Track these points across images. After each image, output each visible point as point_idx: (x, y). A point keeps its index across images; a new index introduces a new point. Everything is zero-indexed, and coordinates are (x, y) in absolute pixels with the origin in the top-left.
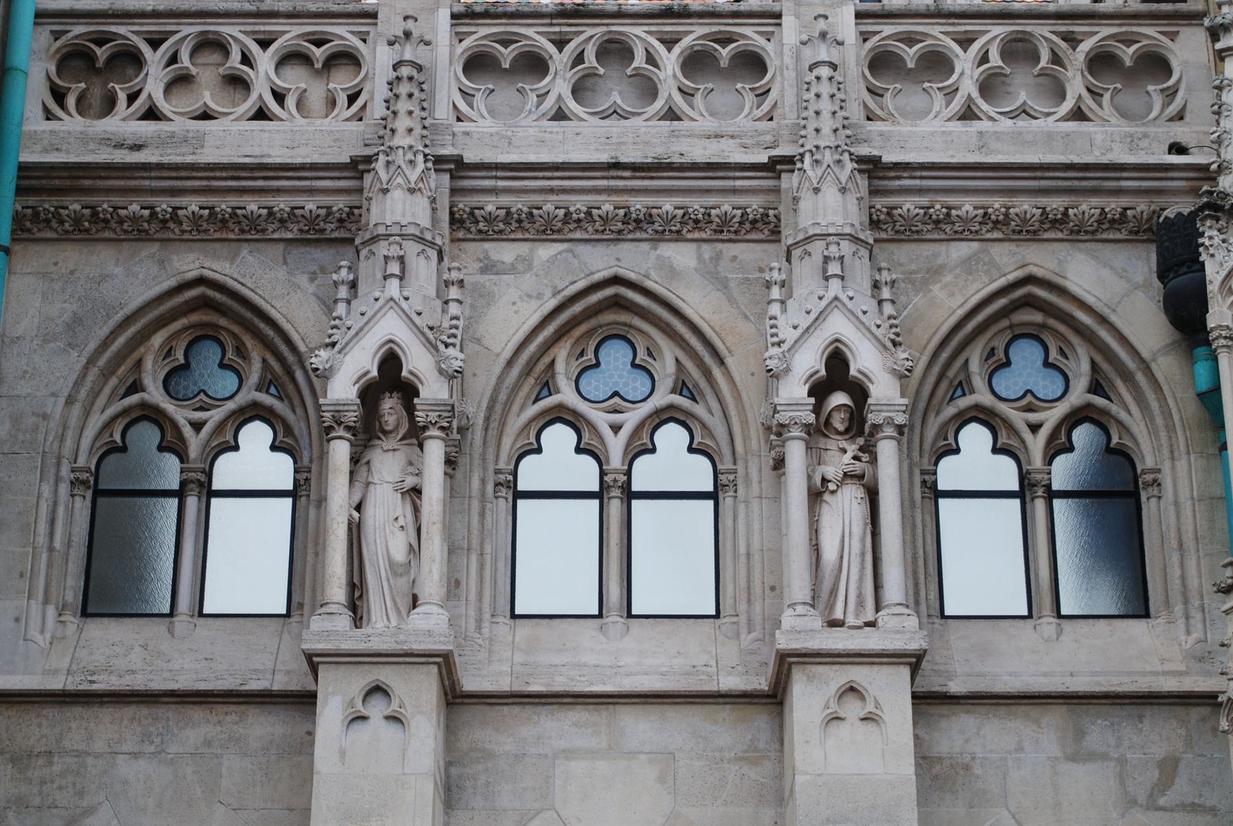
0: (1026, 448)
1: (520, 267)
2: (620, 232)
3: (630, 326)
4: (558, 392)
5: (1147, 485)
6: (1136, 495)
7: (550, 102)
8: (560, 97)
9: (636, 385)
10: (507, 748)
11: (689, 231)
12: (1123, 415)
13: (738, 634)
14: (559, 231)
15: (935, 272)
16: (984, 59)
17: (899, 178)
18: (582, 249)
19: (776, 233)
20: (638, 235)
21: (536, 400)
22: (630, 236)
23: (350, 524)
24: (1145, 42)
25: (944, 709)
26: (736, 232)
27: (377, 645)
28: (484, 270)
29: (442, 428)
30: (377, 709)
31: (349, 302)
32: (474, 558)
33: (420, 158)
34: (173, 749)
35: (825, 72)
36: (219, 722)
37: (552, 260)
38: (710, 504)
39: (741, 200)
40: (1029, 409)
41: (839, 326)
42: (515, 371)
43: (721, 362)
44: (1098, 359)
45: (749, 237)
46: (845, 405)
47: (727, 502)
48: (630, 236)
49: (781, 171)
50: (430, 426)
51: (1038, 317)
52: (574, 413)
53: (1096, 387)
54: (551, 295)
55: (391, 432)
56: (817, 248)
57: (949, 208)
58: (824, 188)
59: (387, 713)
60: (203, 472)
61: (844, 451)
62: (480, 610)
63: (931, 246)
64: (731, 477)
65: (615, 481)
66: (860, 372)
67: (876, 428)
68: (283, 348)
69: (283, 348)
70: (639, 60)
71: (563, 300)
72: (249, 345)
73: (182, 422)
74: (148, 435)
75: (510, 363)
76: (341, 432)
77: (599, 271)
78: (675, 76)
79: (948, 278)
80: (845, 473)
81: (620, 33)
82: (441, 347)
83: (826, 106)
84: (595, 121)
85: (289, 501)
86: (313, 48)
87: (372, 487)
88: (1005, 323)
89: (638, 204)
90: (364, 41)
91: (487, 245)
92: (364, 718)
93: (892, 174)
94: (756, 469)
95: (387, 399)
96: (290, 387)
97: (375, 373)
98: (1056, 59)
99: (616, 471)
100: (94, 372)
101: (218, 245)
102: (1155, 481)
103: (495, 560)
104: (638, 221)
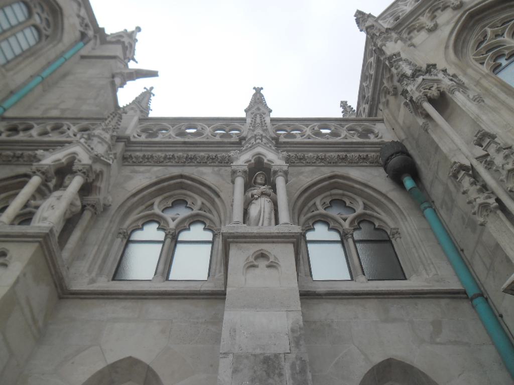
6: (390, 241)
11: (210, 163)
12: (378, 216)
14: (162, 162)
15: (302, 173)
20: (191, 164)
24: (363, 126)
29: (84, 173)
43: (219, 196)
44: (366, 201)
46: (261, 173)
50: (78, 171)
51: (340, 192)
65: (169, 232)
66: (268, 161)
81: (193, 124)
88: (328, 193)
93: (283, 146)
102: (397, 232)
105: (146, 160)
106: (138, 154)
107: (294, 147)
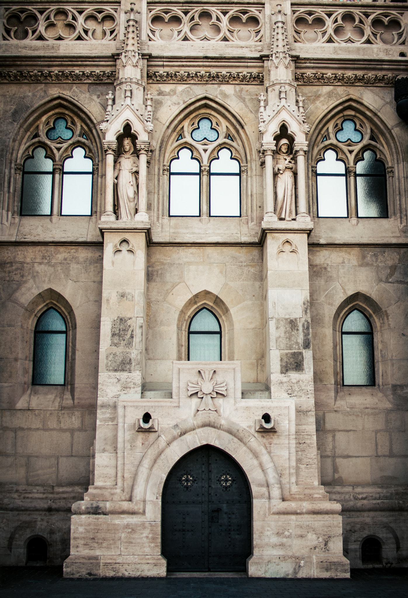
0: (348, 159)
1: (172, 93)
2: (207, 81)
3: (210, 114)
4: (185, 137)
5: (389, 172)
6: (385, 176)
7: (182, 34)
8: (186, 32)
9: (212, 135)
10: (168, 261)
12: (381, 148)
13: (248, 223)
14: (186, 80)
15: (318, 97)
16: (336, 21)
17: (305, 63)
18: (193, 87)
19: (262, 82)
20: (213, 82)
21: (177, 140)
22: (211, 83)
24: (392, 16)
25: (318, 249)
26: (248, 81)
27: (123, 226)
28: (159, 94)
30: (124, 248)
31: (265, 107)
32: (156, 196)
33: (137, 54)
34: (54, 261)
35: (280, 25)
36: (69, 252)
37: (183, 91)
38: (238, 177)
39: (250, 70)
40: (349, 145)
41: (284, 116)
42: (170, 131)
43: (243, 127)
44: (373, 128)
45: (252, 83)
47: (244, 176)
48: (211, 83)
49: (264, 60)
51: (353, 113)
52: (191, 145)
53: (372, 138)
55: (127, 152)
56: (277, 87)
57: (323, 74)
58: (279, 67)
59: (128, 249)
60: (61, 165)
61: (286, 160)
62: (158, 215)
63: (317, 88)
64: (246, 168)
65: (205, 169)
66: (292, 132)
67: (297, 151)
68: (88, 121)
69: (88, 121)
70: (214, 20)
72: (76, 121)
73: (53, 148)
74: (41, 153)
75: (168, 127)
76: (110, 152)
78: (227, 25)
79: (322, 99)
80: (286, 167)
81: (207, 9)
82: (145, 122)
83: (280, 37)
84: (198, 41)
85: (91, 175)
86: (98, 14)
87: (121, 171)
88: (341, 115)
89: (214, 71)
90: (116, 12)
91: (160, 85)
92: (120, 251)
93: (303, 62)
94: (255, 165)
96: (91, 136)
97: (122, 131)
98: (361, 22)
99: (205, 166)
100: (22, 130)
101: (65, 85)
102: (392, 171)
103: (163, 197)
104: (213, 77)
107: (313, 63)
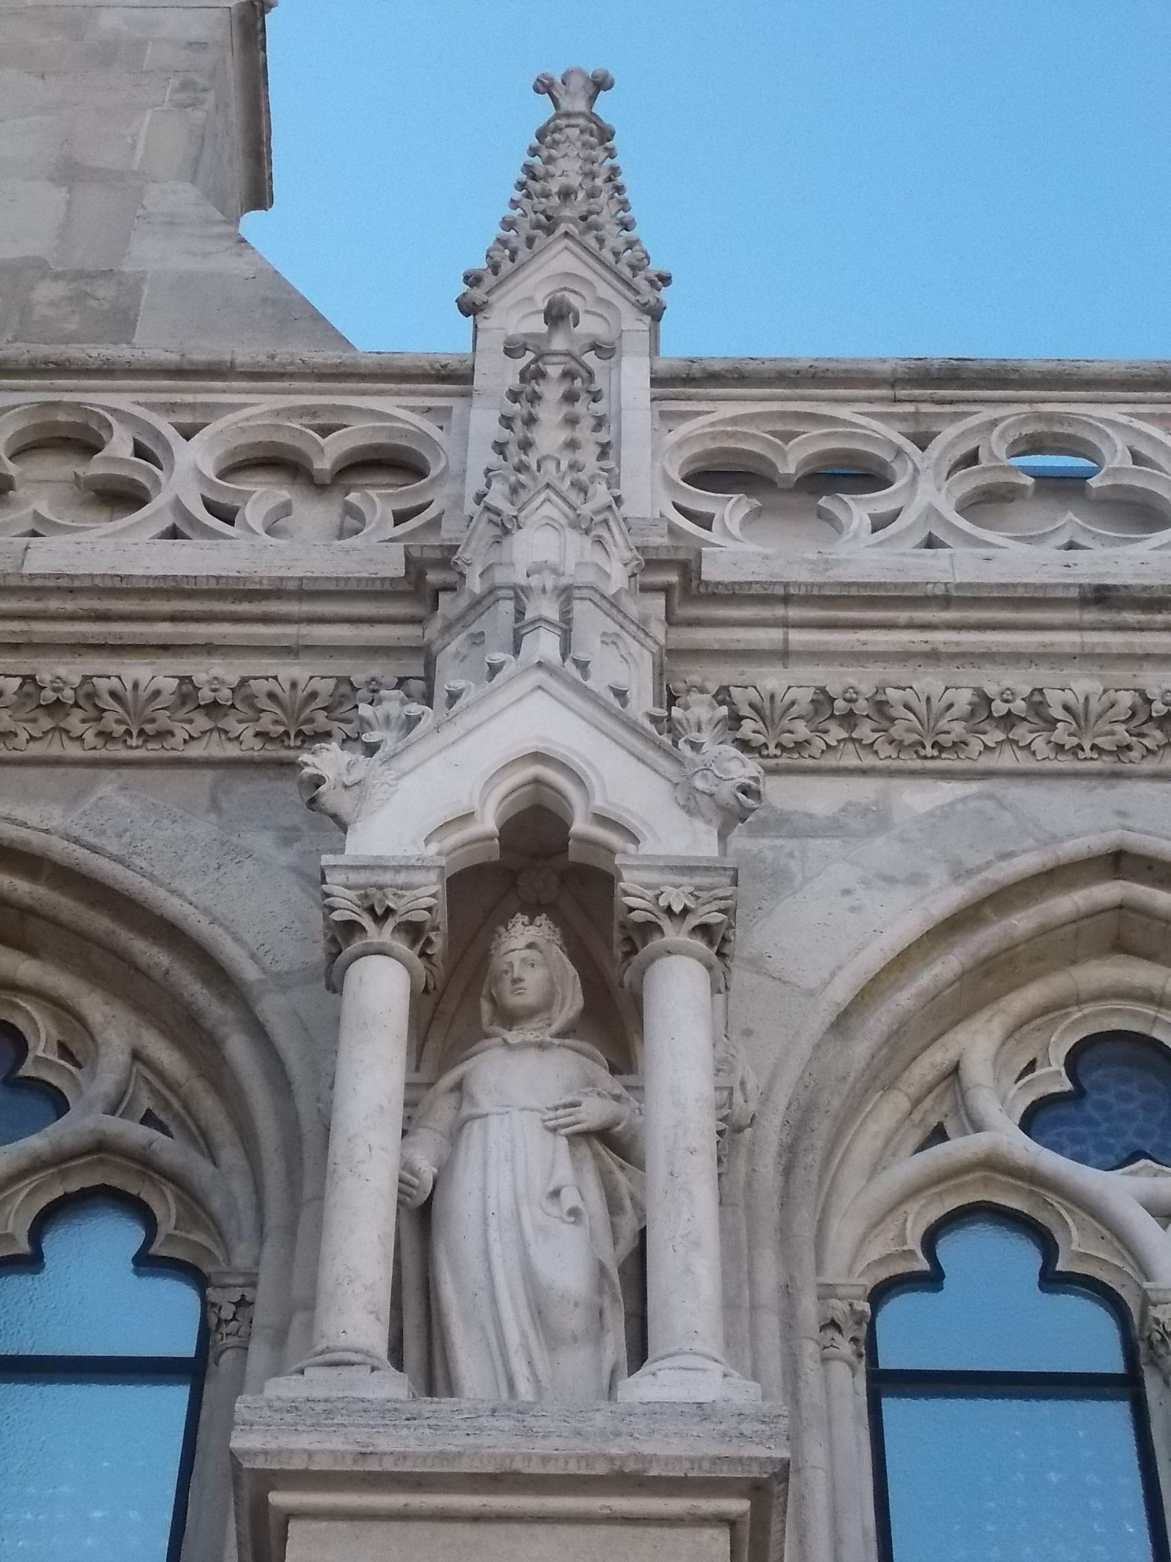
14: (959, 745)
22: (1149, 765)
23: (404, 1187)
29: (704, 930)
37: (946, 813)
48: (1149, 765)
50: (665, 923)
52: (1032, 1178)
54: (946, 878)
55: (530, 1013)
71: (984, 891)
77: (1071, 835)
84: (1022, 548)
95: (519, 926)
97: (489, 823)
105: (837, 733)
106: (772, 680)
